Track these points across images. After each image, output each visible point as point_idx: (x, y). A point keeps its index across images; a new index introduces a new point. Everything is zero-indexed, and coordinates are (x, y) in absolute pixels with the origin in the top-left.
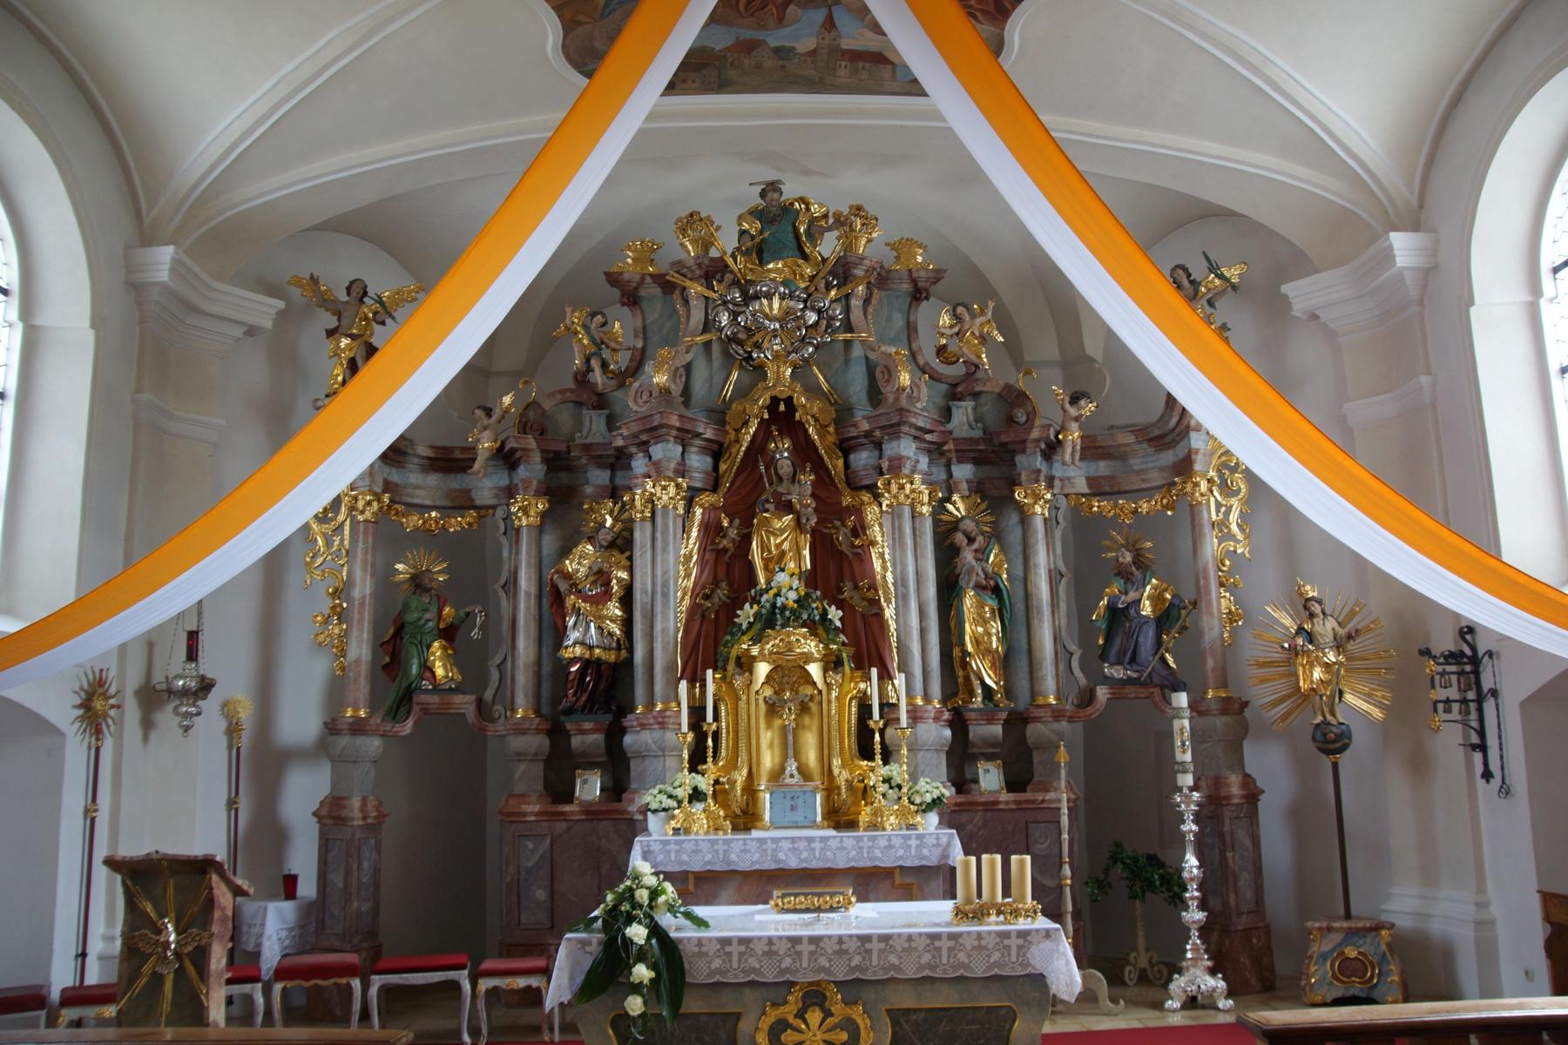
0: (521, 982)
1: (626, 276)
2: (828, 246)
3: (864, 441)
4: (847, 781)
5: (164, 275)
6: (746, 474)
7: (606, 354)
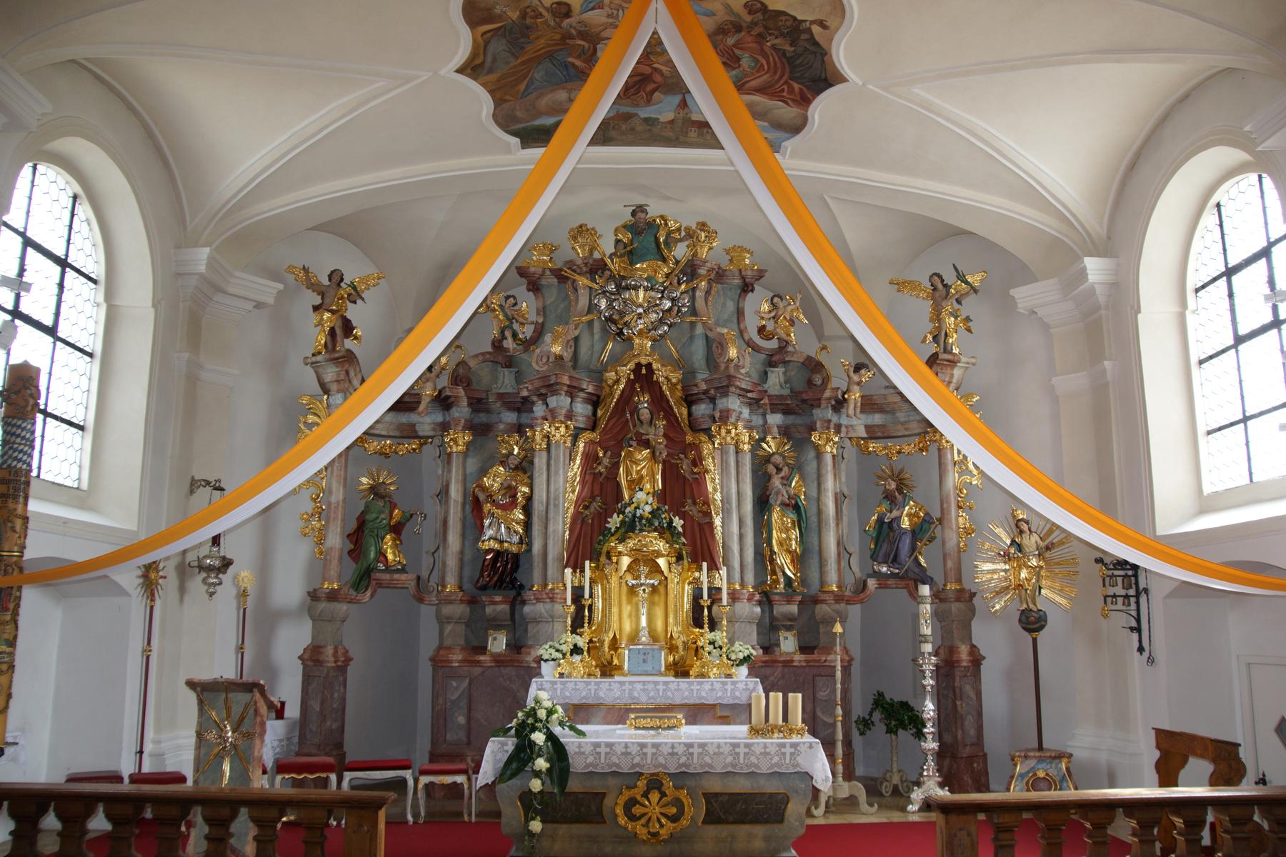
0: (448, 779)
1: (532, 270)
2: (681, 251)
3: (703, 397)
4: (684, 642)
5: (202, 268)
6: (614, 419)
7: (516, 326)
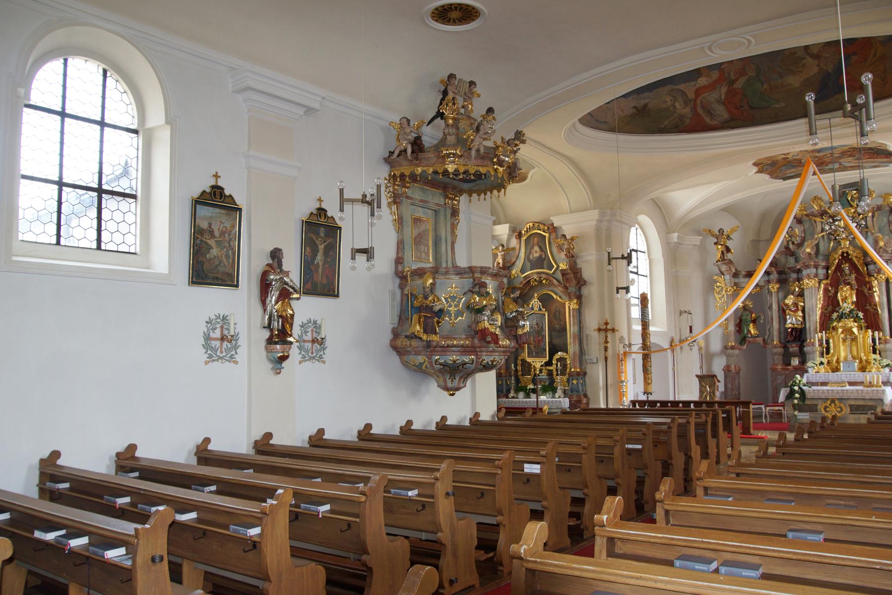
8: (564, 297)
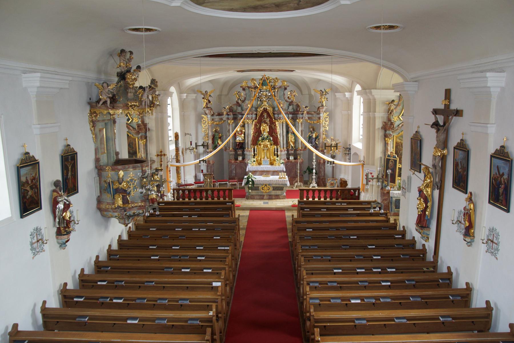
0: (234, 183)
8: (135, 136)
